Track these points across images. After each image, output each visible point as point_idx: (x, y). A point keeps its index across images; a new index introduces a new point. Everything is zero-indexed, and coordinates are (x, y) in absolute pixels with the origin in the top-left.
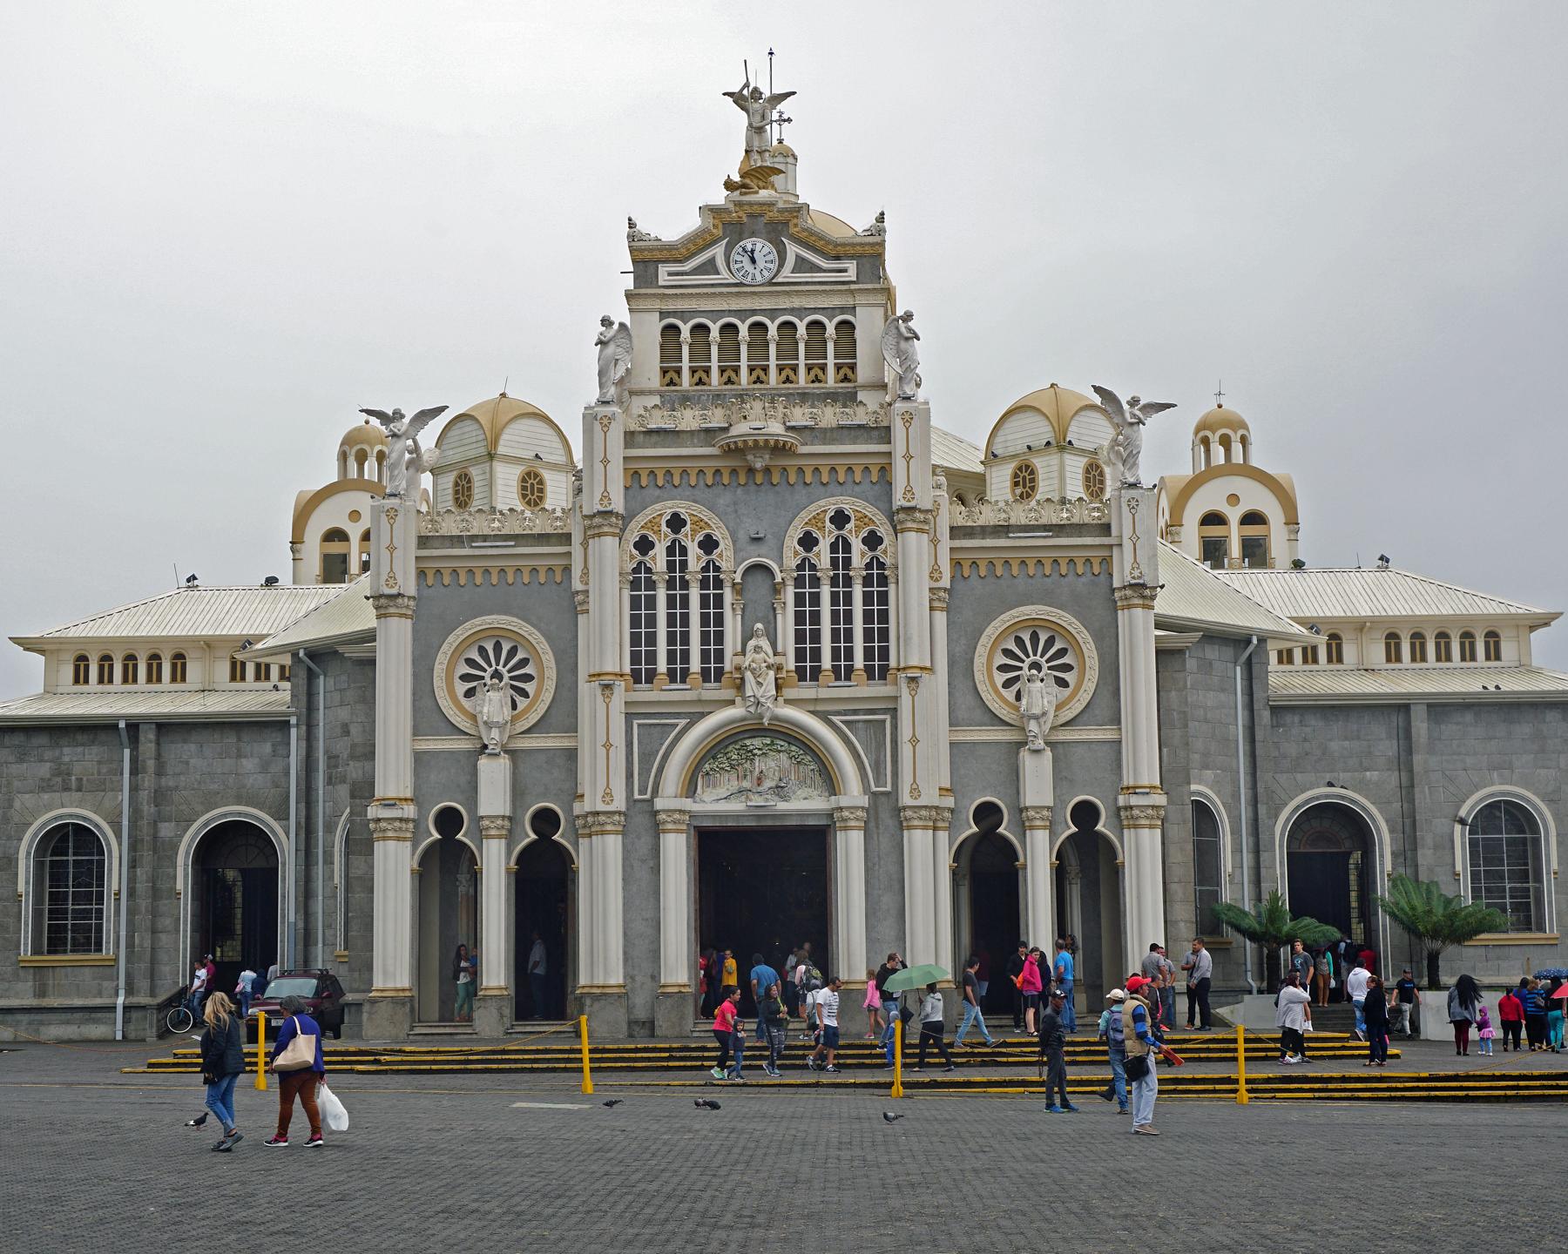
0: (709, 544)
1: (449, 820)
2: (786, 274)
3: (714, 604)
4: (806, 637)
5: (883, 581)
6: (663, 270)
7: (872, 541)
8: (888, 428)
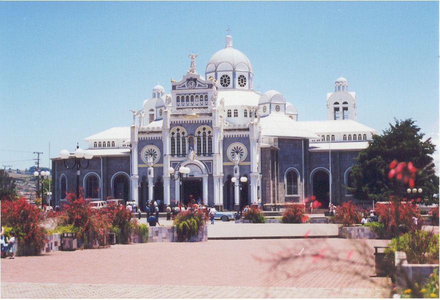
2: (197, 87)
3: (184, 142)
4: (199, 148)
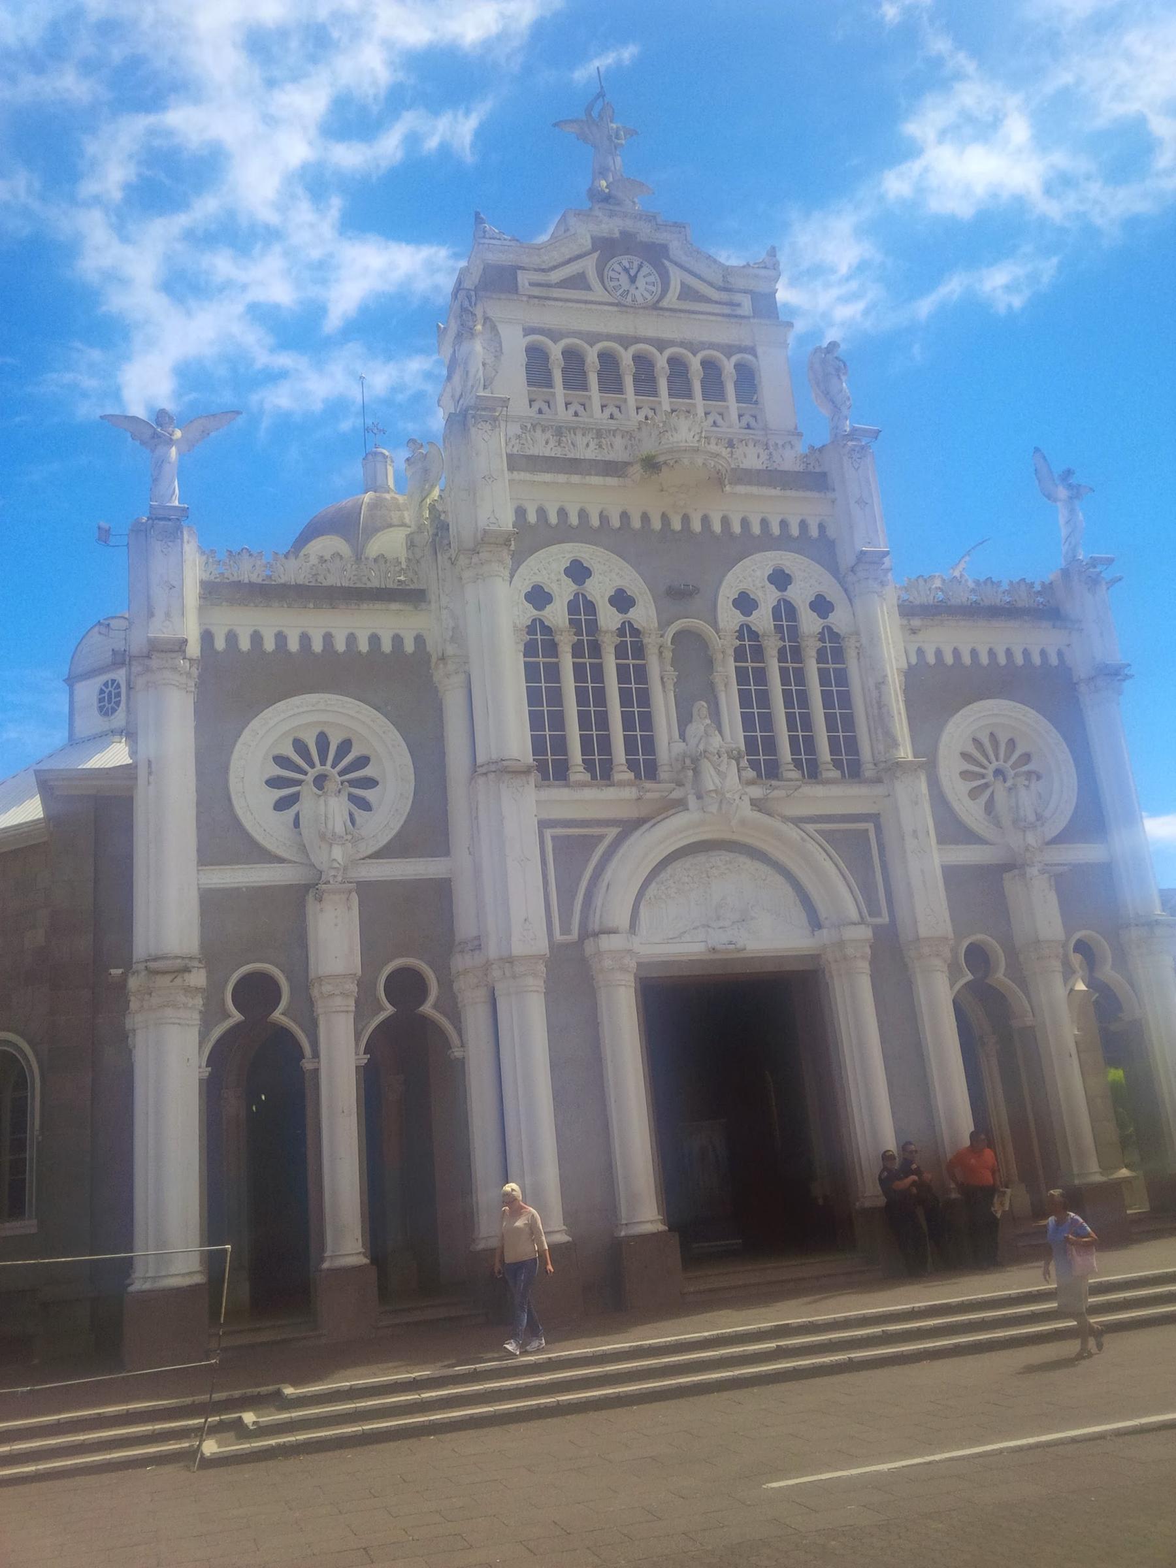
0: (622, 601)
1: (256, 993)
2: (671, 300)
3: (634, 677)
4: (756, 719)
5: (839, 654)
6: (523, 279)
7: (821, 606)
8: (824, 475)
